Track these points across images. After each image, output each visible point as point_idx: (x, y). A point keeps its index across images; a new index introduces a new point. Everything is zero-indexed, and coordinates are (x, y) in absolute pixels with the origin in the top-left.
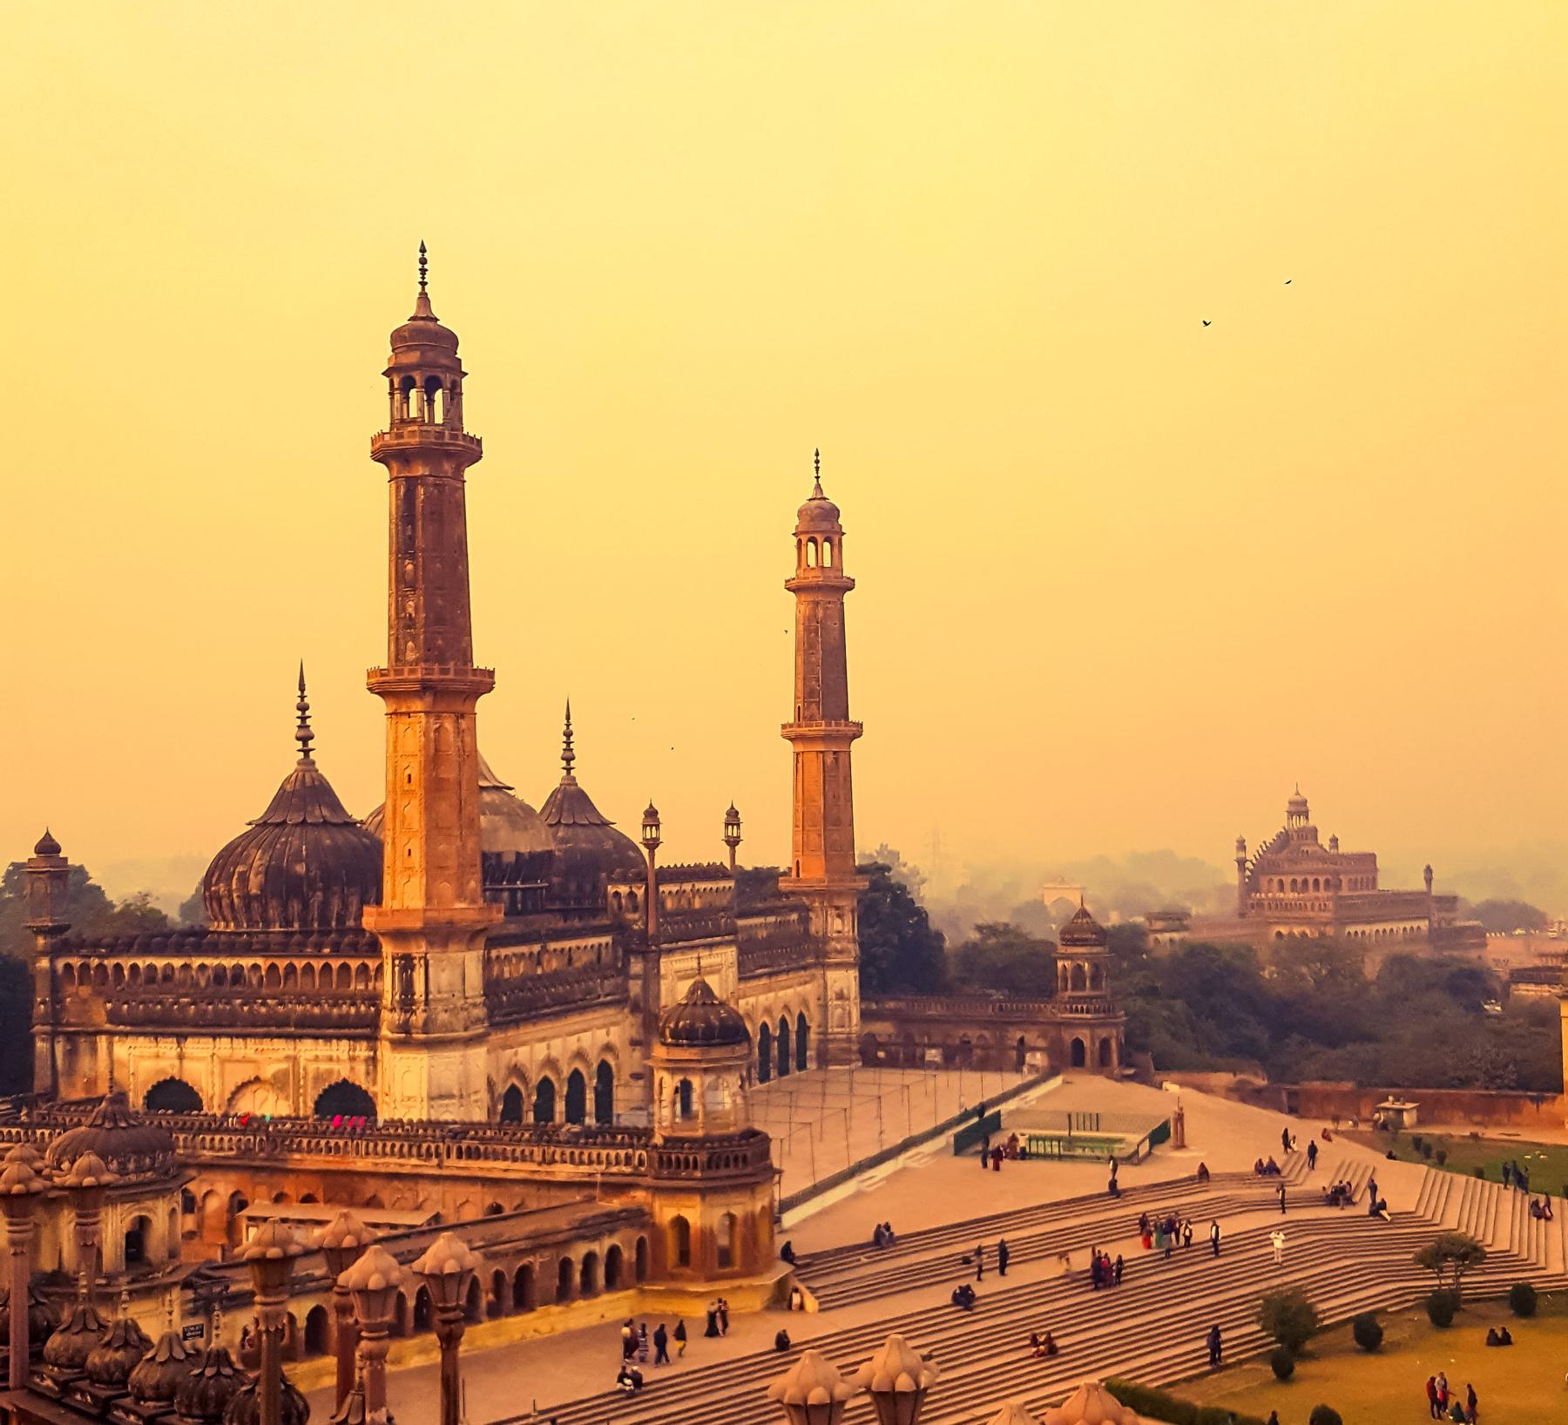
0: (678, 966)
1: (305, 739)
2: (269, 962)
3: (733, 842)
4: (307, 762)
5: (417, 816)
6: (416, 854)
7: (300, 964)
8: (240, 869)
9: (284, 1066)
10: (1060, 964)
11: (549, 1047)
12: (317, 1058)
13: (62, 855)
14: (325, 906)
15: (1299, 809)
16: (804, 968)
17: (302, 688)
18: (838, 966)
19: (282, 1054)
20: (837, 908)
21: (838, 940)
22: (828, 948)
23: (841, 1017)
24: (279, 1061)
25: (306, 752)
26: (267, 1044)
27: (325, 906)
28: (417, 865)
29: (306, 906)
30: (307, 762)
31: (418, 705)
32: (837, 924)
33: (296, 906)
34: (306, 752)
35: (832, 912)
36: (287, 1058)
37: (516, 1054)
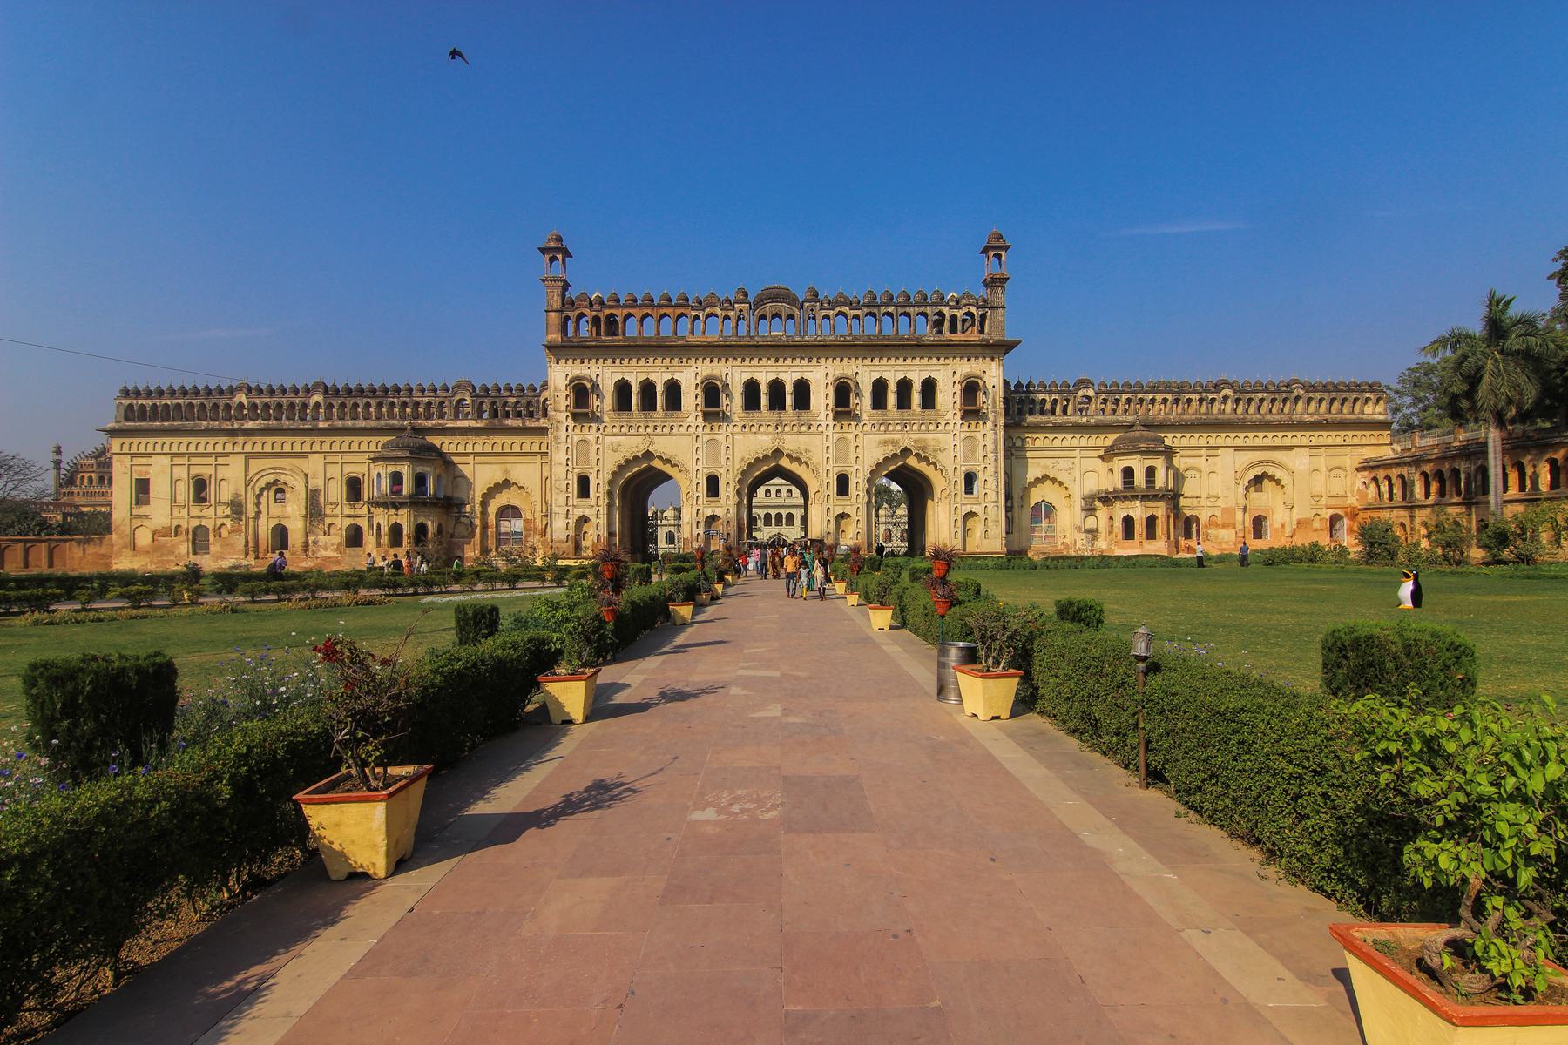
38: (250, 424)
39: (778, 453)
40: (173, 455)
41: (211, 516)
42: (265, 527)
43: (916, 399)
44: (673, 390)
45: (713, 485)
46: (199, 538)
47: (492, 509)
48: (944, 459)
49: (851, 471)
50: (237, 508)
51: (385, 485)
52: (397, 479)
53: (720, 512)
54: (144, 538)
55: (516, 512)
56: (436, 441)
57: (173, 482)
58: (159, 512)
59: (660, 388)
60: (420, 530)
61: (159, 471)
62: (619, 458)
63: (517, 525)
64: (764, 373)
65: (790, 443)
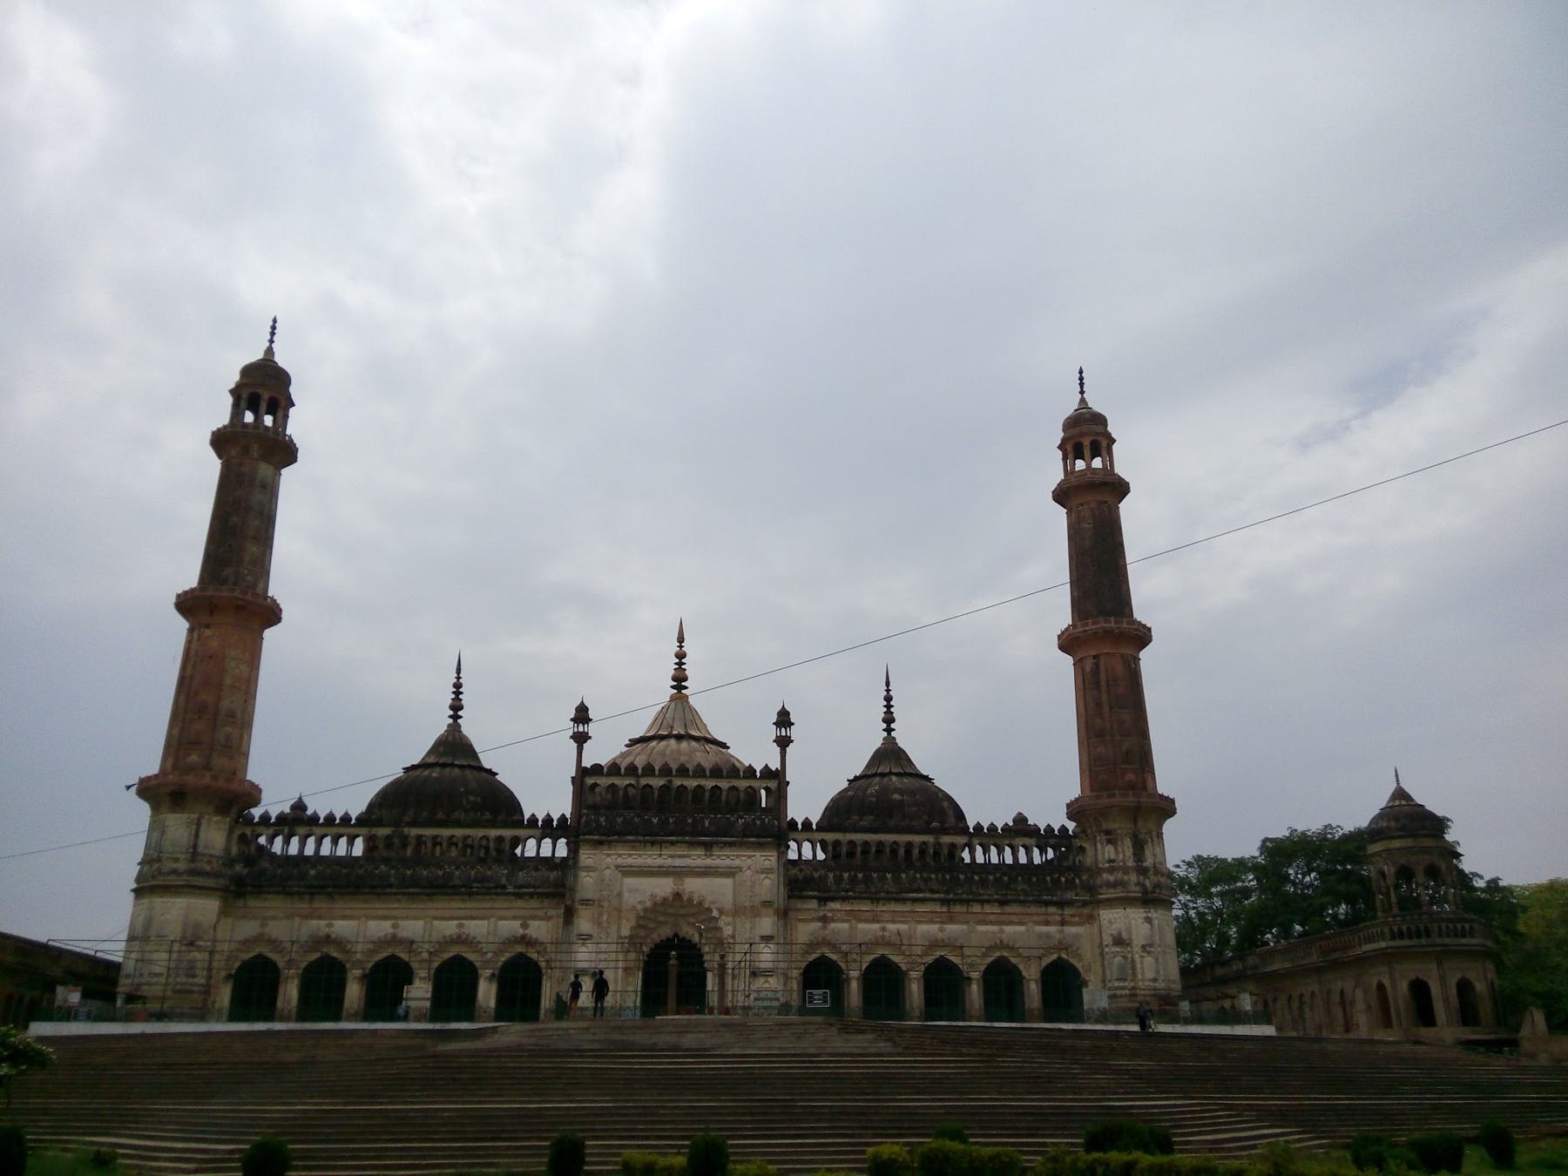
0: (620, 861)
3: (783, 743)
4: (455, 727)
11: (394, 926)
13: (309, 812)
16: (1061, 904)
17: (459, 671)
18: (1111, 903)
20: (1108, 833)
21: (1111, 870)
22: (1098, 881)
23: (1122, 968)
30: (455, 727)
32: (1110, 852)
34: (456, 717)
35: (1101, 838)
37: (330, 926)
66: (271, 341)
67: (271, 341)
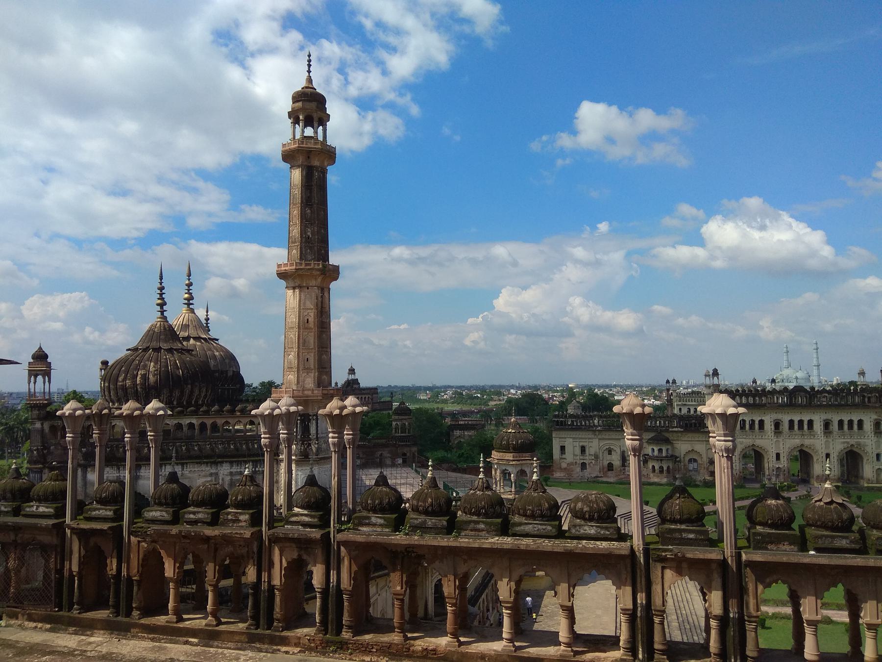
1: (162, 305)
2: (200, 421)
5: (312, 341)
6: (312, 360)
7: (209, 422)
8: (143, 372)
9: (209, 479)
10: (394, 423)
12: (231, 474)
14: (192, 392)
15: (352, 371)
17: (161, 278)
19: (208, 473)
24: (205, 476)
25: (162, 312)
26: (196, 468)
27: (192, 392)
28: (312, 367)
29: (182, 393)
31: (313, 283)
33: (177, 393)
34: (162, 312)
36: (211, 475)
38: (599, 428)
39: (802, 445)
40: (574, 438)
41: (587, 459)
42: (606, 463)
43: (855, 427)
44: (761, 422)
45: (778, 455)
46: (583, 466)
47: (687, 459)
48: (868, 449)
49: (831, 453)
50: (596, 457)
51: (656, 453)
52: (660, 450)
53: (781, 466)
54: (564, 465)
55: (695, 461)
56: (667, 435)
57: (574, 447)
58: (569, 457)
59: (757, 422)
60: (668, 467)
61: (569, 444)
62: (743, 446)
63: (695, 464)
64: (796, 419)
65: (807, 442)
66: (309, 72)
67: (309, 72)
